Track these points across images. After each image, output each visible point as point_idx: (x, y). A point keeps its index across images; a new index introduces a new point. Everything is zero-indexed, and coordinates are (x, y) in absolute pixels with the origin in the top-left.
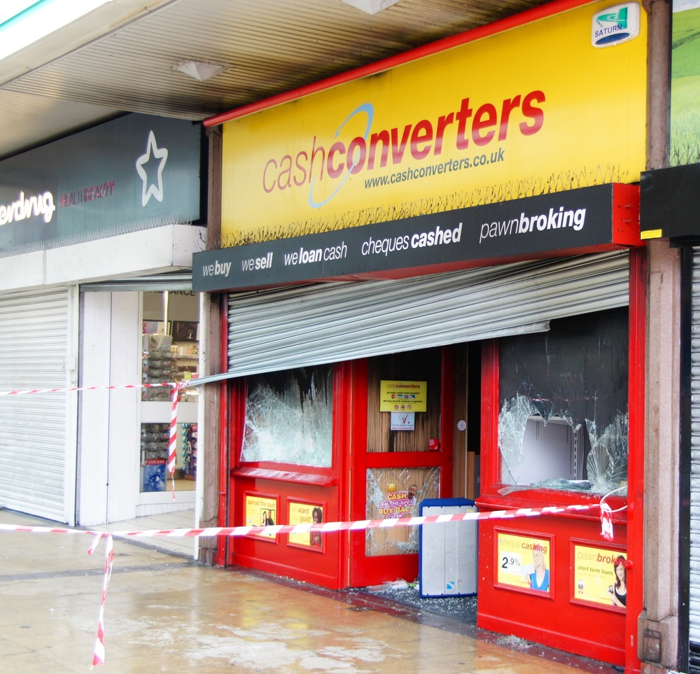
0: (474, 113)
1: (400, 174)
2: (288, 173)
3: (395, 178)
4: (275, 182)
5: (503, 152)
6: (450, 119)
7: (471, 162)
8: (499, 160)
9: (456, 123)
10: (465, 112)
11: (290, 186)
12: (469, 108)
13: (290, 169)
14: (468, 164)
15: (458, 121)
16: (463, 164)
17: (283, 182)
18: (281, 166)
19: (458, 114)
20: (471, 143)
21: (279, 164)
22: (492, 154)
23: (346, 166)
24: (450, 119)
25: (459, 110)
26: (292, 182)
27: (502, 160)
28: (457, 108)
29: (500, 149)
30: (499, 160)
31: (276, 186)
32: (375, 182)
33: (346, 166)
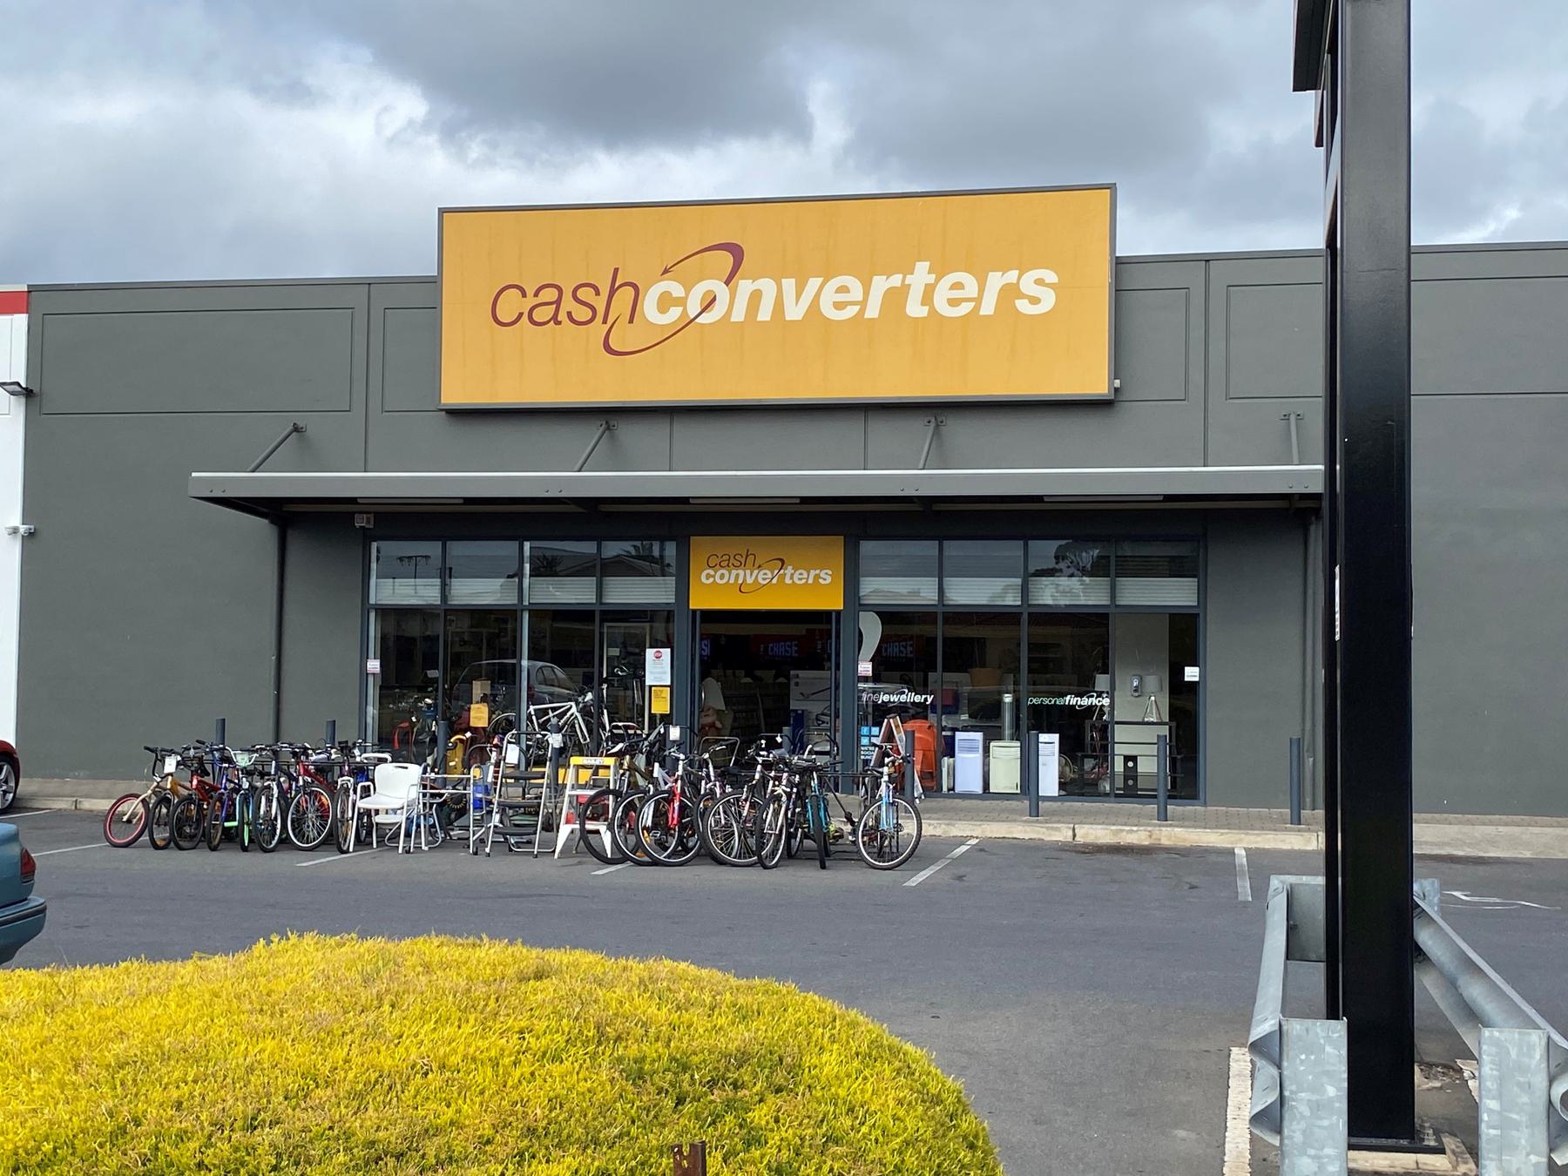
2: (554, 306)
4: (521, 315)
13: (558, 302)
17: (543, 314)
18: (536, 295)
21: (530, 292)
26: (562, 316)
31: (525, 317)
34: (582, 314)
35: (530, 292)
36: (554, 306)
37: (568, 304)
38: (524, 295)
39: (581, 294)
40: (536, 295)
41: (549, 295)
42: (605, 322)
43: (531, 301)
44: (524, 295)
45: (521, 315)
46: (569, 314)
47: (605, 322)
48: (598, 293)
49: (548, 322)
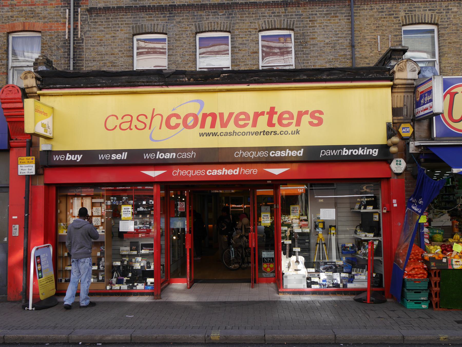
0: (278, 114)
1: (227, 133)
2: (129, 123)
3: (224, 134)
4: (116, 126)
6: (263, 114)
7: (278, 132)
8: (296, 134)
9: (266, 117)
10: (272, 112)
11: (131, 129)
13: (131, 121)
14: (276, 134)
16: (273, 133)
17: (125, 126)
18: (122, 118)
19: (267, 112)
20: (277, 125)
21: (120, 118)
24: (263, 114)
25: (269, 111)
26: (133, 127)
27: (299, 134)
29: (297, 130)
30: (296, 134)
31: (118, 127)
34: (141, 126)
35: (120, 118)
36: (129, 123)
37: (135, 122)
38: (117, 119)
39: (140, 118)
40: (122, 118)
42: (150, 128)
43: (120, 121)
44: (117, 119)
45: (116, 126)
46: (136, 126)
47: (150, 128)
48: (147, 118)
49: (128, 129)
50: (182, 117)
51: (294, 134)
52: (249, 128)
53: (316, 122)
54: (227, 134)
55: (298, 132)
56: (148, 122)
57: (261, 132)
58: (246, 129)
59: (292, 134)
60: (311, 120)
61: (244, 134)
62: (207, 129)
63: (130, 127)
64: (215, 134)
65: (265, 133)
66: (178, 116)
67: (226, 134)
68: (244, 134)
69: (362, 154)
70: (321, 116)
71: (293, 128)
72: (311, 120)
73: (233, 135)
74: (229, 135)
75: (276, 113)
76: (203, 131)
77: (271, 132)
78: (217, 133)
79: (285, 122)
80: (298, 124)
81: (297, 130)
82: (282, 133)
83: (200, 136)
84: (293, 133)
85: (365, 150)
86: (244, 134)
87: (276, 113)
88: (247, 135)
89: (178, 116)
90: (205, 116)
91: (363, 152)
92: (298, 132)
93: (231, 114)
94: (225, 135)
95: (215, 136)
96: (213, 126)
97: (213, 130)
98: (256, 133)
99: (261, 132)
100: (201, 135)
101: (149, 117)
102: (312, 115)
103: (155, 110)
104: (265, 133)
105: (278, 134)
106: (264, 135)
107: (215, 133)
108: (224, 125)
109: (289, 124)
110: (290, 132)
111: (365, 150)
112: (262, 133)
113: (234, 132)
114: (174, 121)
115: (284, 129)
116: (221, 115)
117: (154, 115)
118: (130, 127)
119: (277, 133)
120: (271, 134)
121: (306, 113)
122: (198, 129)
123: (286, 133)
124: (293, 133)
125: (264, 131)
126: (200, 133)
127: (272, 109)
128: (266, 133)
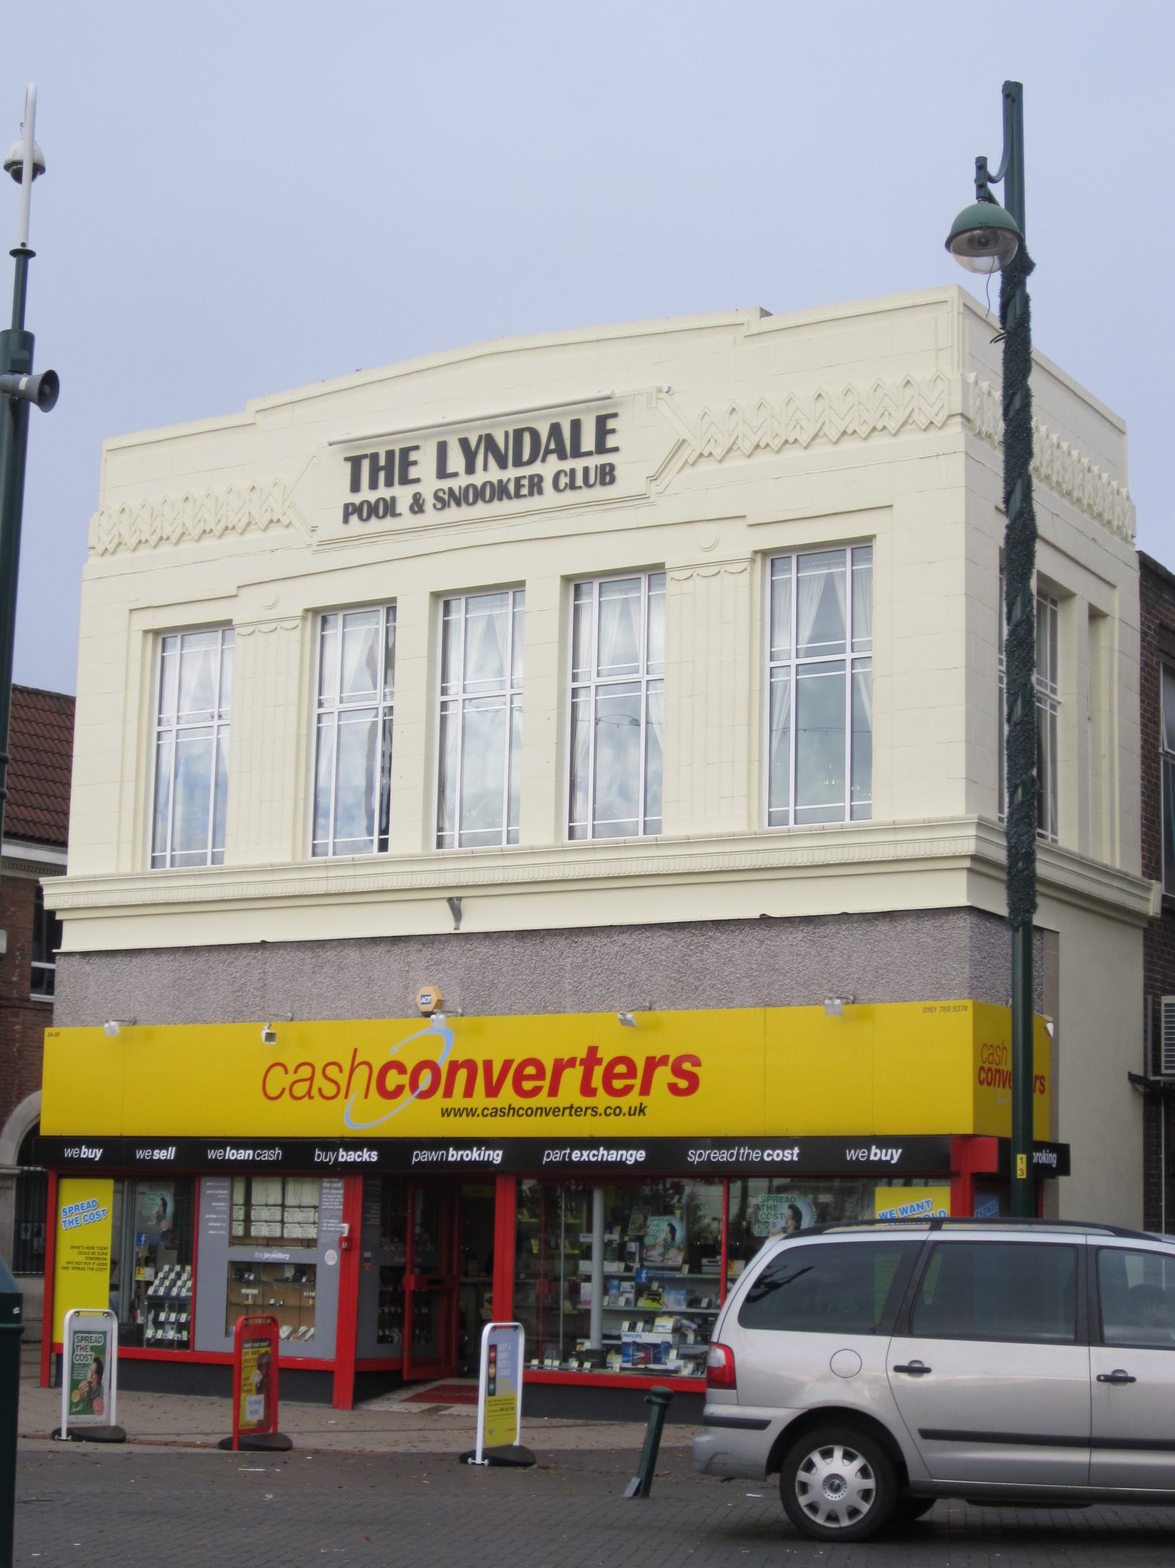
2: (307, 1084)
3: (489, 1112)
4: (283, 1090)
5: (645, 1107)
7: (601, 1110)
8: (639, 1114)
10: (591, 1059)
11: (311, 1098)
12: (599, 1055)
13: (311, 1079)
14: (596, 1113)
15: (582, 1068)
16: (589, 1111)
17: (300, 1090)
20: (601, 1091)
21: (291, 1068)
22: (630, 1108)
23: (407, 1090)
24: (572, 1062)
26: (315, 1092)
27: (644, 1114)
28: (582, 1054)
29: (641, 1104)
30: (639, 1114)
31: (287, 1092)
32: (458, 1112)
33: (407, 1090)
34: (330, 1089)
35: (291, 1068)
36: (307, 1084)
37: (319, 1081)
38: (286, 1072)
40: (296, 1071)
41: (305, 1072)
42: (346, 1096)
43: (292, 1077)
44: (286, 1072)
45: (283, 1090)
46: (320, 1090)
47: (346, 1096)
48: (341, 1070)
49: (304, 1097)
50: (410, 1068)
51: (634, 1114)
52: (542, 1100)
53: (683, 1084)
54: (496, 1112)
55: (642, 1110)
56: (342, 1079)
57: (564, 1109)
58: (534, 1102)
59: (630, 1114)
60: (674, 1080)
61: (529, 1112)
62: (458, 1100)
63: (309, 1092)
64: (471, 1112)
65: (574, 1111)
66: (401, 1068)
67: (495, 1112)
68: (529, 1112)
69: (478, 1159)
70: (695, 1070)
71: (633, 1099)
72: (674, 1080)
73: (508, 1115)
74: (500, 1115)
75: (599, 1062)
76: (449, 1103)
77: (587, 1109)
78: (476, 1109)
79: (618, 1084)
80: (645, 1090)
81: (641, 1104)
82: (609, 1111)
83: (443, 1115)
84: (632, 1112)
85: (483, 1153)
86: (531, 1112)
87: (599, 1062)
88: (536, 1115)
89: (401, 1068)
90: (454, 1067)
91: (479, 1155)
92: (642, 1110)
93: (507, 1064)
94: (491, 1115)
95: (473, 1115)
96: (469, 1092)
97: (469, 1103)
98: (554, 1112)
99: (564, 1109)
100: (445, 1113)
101: (347, 1068)
102: (678, 1071)
103: (358, 1054)
104: (574, 1111)
105: (600, 1115)
106: (570, 1115)
107: (472, 1109)
108: (492, 1090)
109: (627, 1090)
110: (625, 1110)
111: (483, 1153)
112: (567, 1111)
113: (510, 1109)
114: (393, 1079)
115: (614, 1102)
116: (488, 1065)
117: (356, 1063)
118: (309, 1092)
119: (599, 1112)
120: (585, 1114)
121: (664, 1060)
122: (438, 1099)
123: (618, 1111)
124: (632, 1112)
125: (571, 1107)
126: (442, 1109)
127: (593, 1051)
128: (576, 1111)
